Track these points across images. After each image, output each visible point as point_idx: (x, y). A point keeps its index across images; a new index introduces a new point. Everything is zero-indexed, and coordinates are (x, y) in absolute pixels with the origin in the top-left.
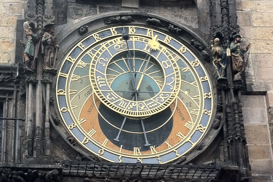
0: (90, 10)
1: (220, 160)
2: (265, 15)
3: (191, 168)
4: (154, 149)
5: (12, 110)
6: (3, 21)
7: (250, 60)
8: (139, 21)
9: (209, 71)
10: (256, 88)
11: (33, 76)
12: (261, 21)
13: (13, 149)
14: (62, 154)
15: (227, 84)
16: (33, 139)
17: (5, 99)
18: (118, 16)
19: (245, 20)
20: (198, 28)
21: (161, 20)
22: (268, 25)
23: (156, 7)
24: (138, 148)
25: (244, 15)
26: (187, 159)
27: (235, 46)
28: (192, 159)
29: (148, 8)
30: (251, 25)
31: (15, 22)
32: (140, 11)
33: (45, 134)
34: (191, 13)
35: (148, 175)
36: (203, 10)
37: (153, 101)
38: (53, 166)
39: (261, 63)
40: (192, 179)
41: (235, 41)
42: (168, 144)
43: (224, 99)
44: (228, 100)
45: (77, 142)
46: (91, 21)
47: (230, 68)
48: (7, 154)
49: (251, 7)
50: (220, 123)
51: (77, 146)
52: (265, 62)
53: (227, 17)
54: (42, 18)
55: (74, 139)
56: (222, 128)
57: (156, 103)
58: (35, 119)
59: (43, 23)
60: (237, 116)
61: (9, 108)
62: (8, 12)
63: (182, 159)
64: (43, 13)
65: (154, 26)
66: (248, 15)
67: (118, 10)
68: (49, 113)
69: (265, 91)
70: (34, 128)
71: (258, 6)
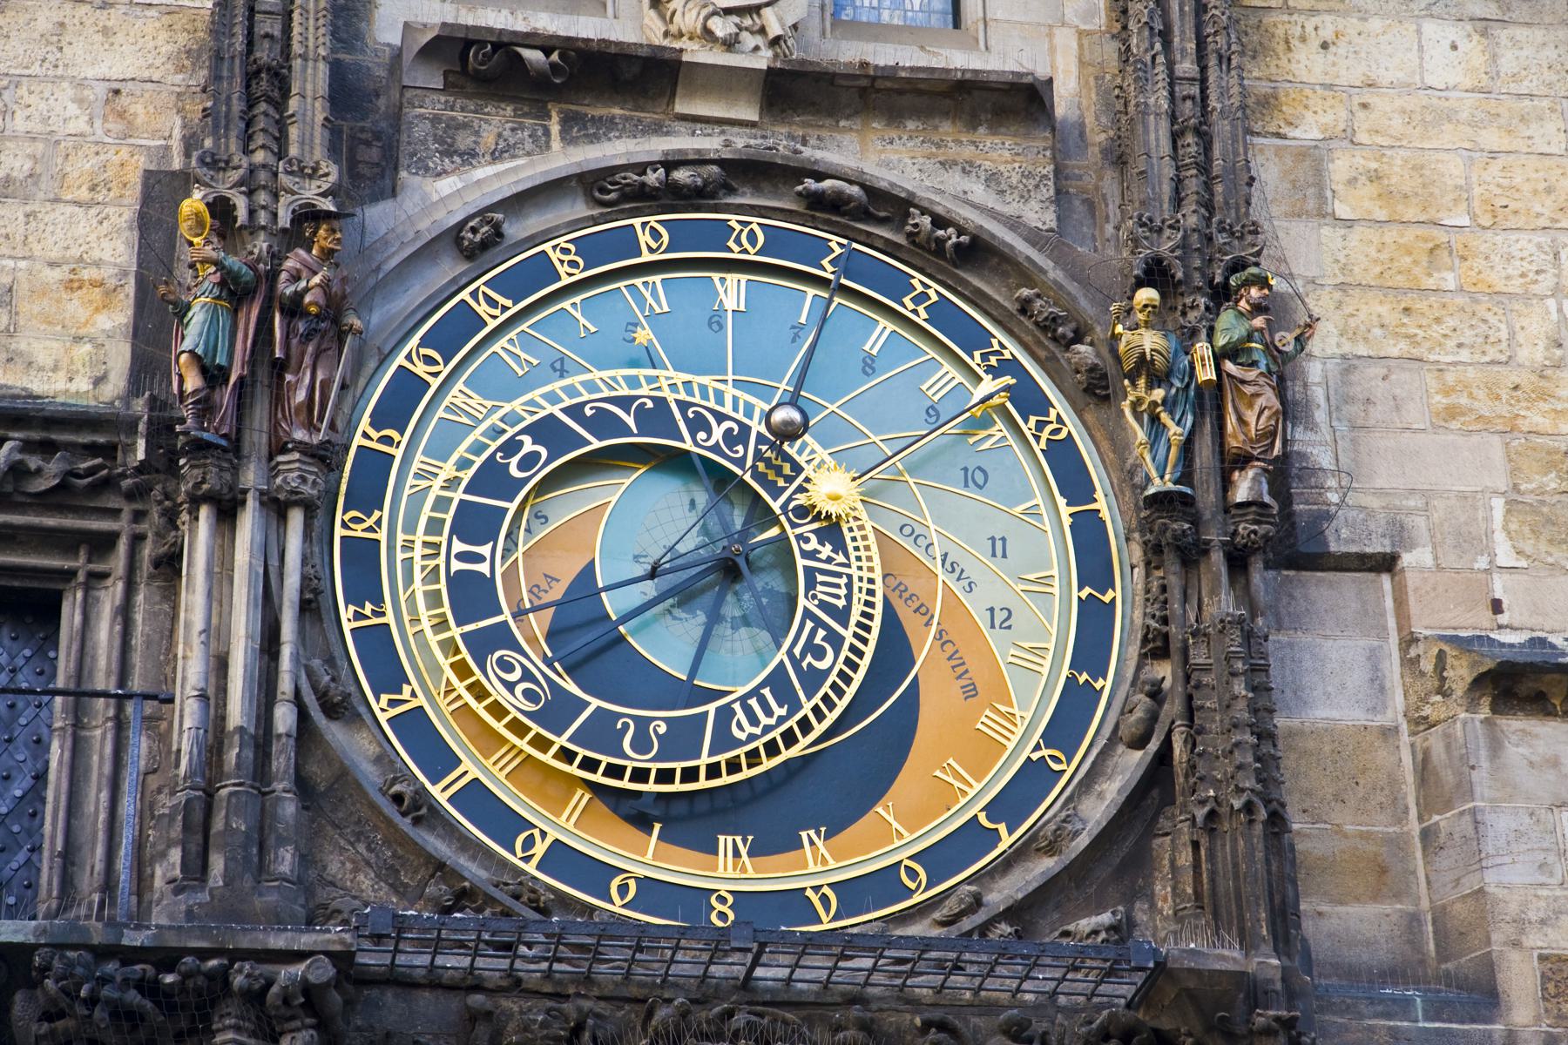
0: (513, 130)
1: (1153, 905)
2: (1399, 162)
3: (1004, 953)
4: (819, 843)
5: (104, 632)
6: (76, 174)
7: (1318, 394)
8: (758, 190)
10: (1344, 533)
12: (1372, 189)
13: (101, 836)
14: (356, 870)
15: (1196, 521)
16: (210, 794)
17: (72, 574)
18: (653, 165)
19: (1293, 182)
20: (1054, 225)
21: (872, 192)
22: (1411, 213)
23: (848, 118)
25: (1289, 161)
27: (1239, 332)
28: (1011, 902)
29: (804, 124)
30: (1323, 213)
31: (135, 179)
32: (764, 137)
33: (274, 764)
35: (789, 980)
38: (305, 941)
39: (1371, 409)
40: (1011, 1007)
41: (1243, 303)
42: (891, 819)
43: (1175, 594)
46: (520, 188)
47: (1208, 439)
48: (73, 864)
49: (1328, 119)
50: (1153, 718)
51: (432, 828)
53: (1203, 178)
54: (276, 174)
55: (416, 792)
58: (222, 690)
59: (276, 196)
60: (1239, 688)
62: (99, 132)
63: (961, 901)
64: (280, 131)
65: (834, 218)
67: (658, 129)
68: (296, 658)
69: (1388, 550)
70: (216, 737)
71: (1361, 114)
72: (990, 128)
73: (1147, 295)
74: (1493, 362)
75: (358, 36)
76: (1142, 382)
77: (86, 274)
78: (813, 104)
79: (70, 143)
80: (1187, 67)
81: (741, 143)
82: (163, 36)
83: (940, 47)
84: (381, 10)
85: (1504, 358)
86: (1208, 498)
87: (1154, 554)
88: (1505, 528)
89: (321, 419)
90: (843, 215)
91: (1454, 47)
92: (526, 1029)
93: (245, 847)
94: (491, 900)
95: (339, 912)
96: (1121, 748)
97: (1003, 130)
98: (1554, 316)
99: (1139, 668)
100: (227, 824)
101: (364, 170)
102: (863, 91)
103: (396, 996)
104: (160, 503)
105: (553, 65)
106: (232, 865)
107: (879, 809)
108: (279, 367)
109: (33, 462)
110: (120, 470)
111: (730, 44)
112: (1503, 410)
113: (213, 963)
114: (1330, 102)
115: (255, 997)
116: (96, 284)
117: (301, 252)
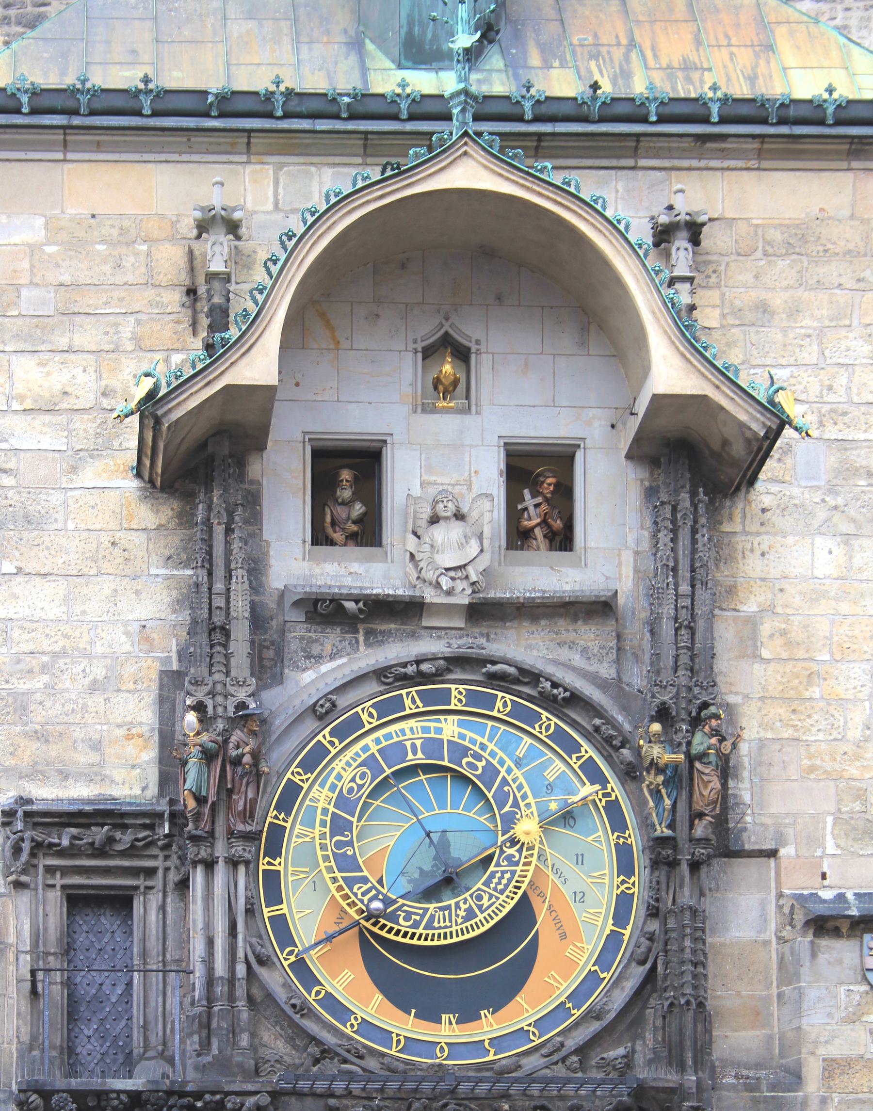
1: (644, 1042)
8: (464, 669)
18: (410, 663)
21: (521, 670)
26: (566, 1043)
34: (598, 633)
42: (523, 1003)
51: (309, 1018)
54: (225, 685)
56: (655, 964)
59: (226, 697)
74: (835, 740)
76: (653, 772)
79: (123, 657)
85: (840, 737)
86: (682, 834)
87: (655, 864)
88: (832, 833)
90: (506, 681)
91: (830, 553)
96: (634, 964)
98: (868, 712)
99: (645, 923)
102: (518, 608)
105: (360, 610)
107: (518, 998)
108: (230, 792)
112: (837, 766)
114: (764, 588)
117: (239, 732)
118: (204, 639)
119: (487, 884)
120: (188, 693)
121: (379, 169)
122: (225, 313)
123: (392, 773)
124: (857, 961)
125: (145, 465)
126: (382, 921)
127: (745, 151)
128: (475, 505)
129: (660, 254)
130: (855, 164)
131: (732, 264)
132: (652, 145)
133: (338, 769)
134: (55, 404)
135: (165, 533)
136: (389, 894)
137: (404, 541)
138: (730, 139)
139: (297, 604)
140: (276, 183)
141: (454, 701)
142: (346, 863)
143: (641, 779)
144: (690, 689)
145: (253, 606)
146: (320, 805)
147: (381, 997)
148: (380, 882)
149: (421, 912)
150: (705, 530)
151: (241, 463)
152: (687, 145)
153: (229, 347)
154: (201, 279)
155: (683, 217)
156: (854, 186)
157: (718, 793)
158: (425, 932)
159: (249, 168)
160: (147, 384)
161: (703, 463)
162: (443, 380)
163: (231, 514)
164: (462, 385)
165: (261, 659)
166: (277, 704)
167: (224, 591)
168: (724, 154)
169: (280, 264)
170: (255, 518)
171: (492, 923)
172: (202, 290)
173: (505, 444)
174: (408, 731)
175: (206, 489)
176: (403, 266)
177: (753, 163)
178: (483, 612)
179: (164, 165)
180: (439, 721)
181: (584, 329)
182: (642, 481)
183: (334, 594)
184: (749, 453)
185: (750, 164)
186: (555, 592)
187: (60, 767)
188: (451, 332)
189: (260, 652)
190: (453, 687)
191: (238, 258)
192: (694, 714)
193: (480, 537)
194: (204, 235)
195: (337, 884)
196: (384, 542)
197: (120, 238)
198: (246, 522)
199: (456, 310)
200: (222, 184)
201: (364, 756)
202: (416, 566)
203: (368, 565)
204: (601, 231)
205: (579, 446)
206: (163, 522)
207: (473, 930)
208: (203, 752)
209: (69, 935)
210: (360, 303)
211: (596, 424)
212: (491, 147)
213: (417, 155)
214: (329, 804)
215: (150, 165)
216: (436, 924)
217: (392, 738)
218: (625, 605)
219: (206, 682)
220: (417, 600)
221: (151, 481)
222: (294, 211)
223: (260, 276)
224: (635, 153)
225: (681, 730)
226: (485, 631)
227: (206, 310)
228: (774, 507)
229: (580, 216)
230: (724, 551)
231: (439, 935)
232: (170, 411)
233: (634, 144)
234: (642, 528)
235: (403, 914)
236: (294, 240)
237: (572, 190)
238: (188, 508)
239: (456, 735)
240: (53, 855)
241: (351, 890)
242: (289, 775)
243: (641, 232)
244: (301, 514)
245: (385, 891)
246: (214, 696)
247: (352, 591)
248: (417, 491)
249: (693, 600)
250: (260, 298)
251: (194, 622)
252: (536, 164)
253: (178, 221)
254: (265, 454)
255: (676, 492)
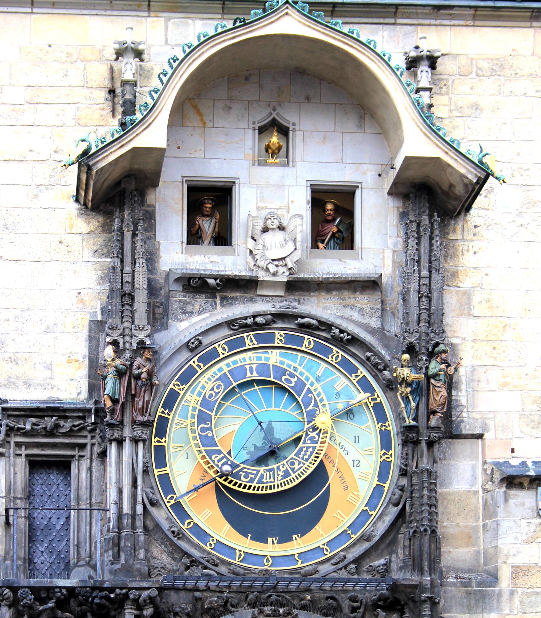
0: (205, 303)
5: (84, 474)
8: (283, 321)
9: (392, 404)
11: (118, 430)
13: (88, 540)
14: (162, 553)
16: (120, 533)
17: (73, 456)
18: (249, 317)
19: (461, 303)
21: (320, 322)
23: (313, 292)
24: (274, 539)
25: (460, 295)
36: (392, 288)
37: (304, 447)
44: (418, 458)
45: (183, 534)
51: (183, 540)
52: (486, 381)
53: (428, 313)
54: (131, 330)
57: (310, 447)
59: (131, 337)
61: (81, 471)
65: (308, 330)
66: (466, 296)
67: (251, 300)
68: (142, 490)
72: (360, 292)
73: (406, 356)
75: (155, 268)
77: (72, 358)
78: (302, 288)
80: (425, 273)
81: (278, 306)
82: (94, 272)
83: (346, 259)
84: (162, 258)
89: (146, 412)
92: (211, 603)
93: (130, 551)
94: (201, 563)
95: (157, 568)
97: (364, 293)
100: (125, 544)
101: (157, 316)
102: (318, 284)
103: (174, 592)
104: (99, 434)
105: (217, 284)
106: (127, 556)
109: (62, 423)
110: (86, 424)
111: (275, 274)
113: (124, 591)
115: (136, 601)
116: (77, 361)
118: (118, 301)
119: (297, 455)
120: (107, 335)
121: (232, 22)
122: (133, 104)
123: (237, 385)
124: (534, 504)
125: (81, 195)
126: (230, 478)
127: (464, 15)
128: (292, 221)
129: (410, 74)
130: (535, 24)
131: (456, 81)
132: (406, 11)
133: (203, 382)
134: (24, 157)
135: (94, 236)
136: (234, 461)
137: (246, 242)
138: (456, 8)
139: (178, 280)
140: (167, 28)
141: (277, 341)
142: (208, 441)
143: (397, 390)
144: (428, 334)
145: (149, 281)
146: (191, 405)
147: (229, 526)
148: (229, 453)
149: (255, 472)
150: (438, 238)
151: (142, 194)
152: (428, 11)
153: (135, 125)
154: (118, 85)
155: (425, 53)
156: (534, 36)
157: (445, 399)
158: (257, 485)
159: (149, 19)
160: (83, 146)
161: (436, 198)
162: (272, 147)
163: (135, 225)
164: (284, 149)
165: (154, 314)
166: (164, 342)
167: (131, 272)
168: (452, 17)
169: (168, 76)
170: (151, 227)
171: (300, 479)
172: (118, 91)
173: (311, 185)
174: (247, 359)
175: (120, 210)
176: (247, 79)
177: (470, 23)
178: (296, 286)
179: (95, 17)
180: (267, 353)
181: (362, 118)
182: (398, 208)
183: (201, 274)
184: (467, 192)
185: (468, 23)
186: (342, 274)
187: (25, 379)
188: (277, 118)
189: (153, 309)
190: (277, 332)
191: (141, 72)
192: (430, 350)
193: (295, 241)
194: (120, 58)
195: (201, 455)
196: (233, 243)
197: (67, 59)
198: (145, 230)
199: (280, 105)
200: (132, 29)
201: (219, 374)
202: (254, 258)
203: (222, 257)
204: (373, 60)
205: (358, 187)
206: (92, 229)
207: (288, 484)
208: (116, 371)
209: (30, 486)
210: (219, 100)
211: (369, 174)
212: (303, 10)
213: (256, 14)
214: (197, 404)
215: (86, 17)
216: (264, 480)
217: (237, 363)
218: (387, 283)
219: (119, 327)
220: (254, 279)
221: (85, 204)
222: (177, 45)
223: (155, 83)
224: (395, 15)
225: (422, 360)
226: (297, 298)
227: (121, 102)
228: (482, 225)
229: (360, 51)
230: (449, 250)
231: (267, 487)
232: (97, 162)
233: (394, 10)
234: (398, 236)
235: (243, 474)
236: (178, 62)
237: (355, 36)
238: (108, 221)
239: (278, 362)
240: (20, 435)
241: (210, 458)
242: (171, 386)
243: (399, 62)
244: (181, 225)
245: (232, 459)
246: (124, 336)
247: (213, 273)
248: (254, 213)
249: (430, 280)
250: (156, 96)
251: (112, 291)
252: (332, 21)
253: (103, 50)
254: (158, 189)
255: (420, 215)
